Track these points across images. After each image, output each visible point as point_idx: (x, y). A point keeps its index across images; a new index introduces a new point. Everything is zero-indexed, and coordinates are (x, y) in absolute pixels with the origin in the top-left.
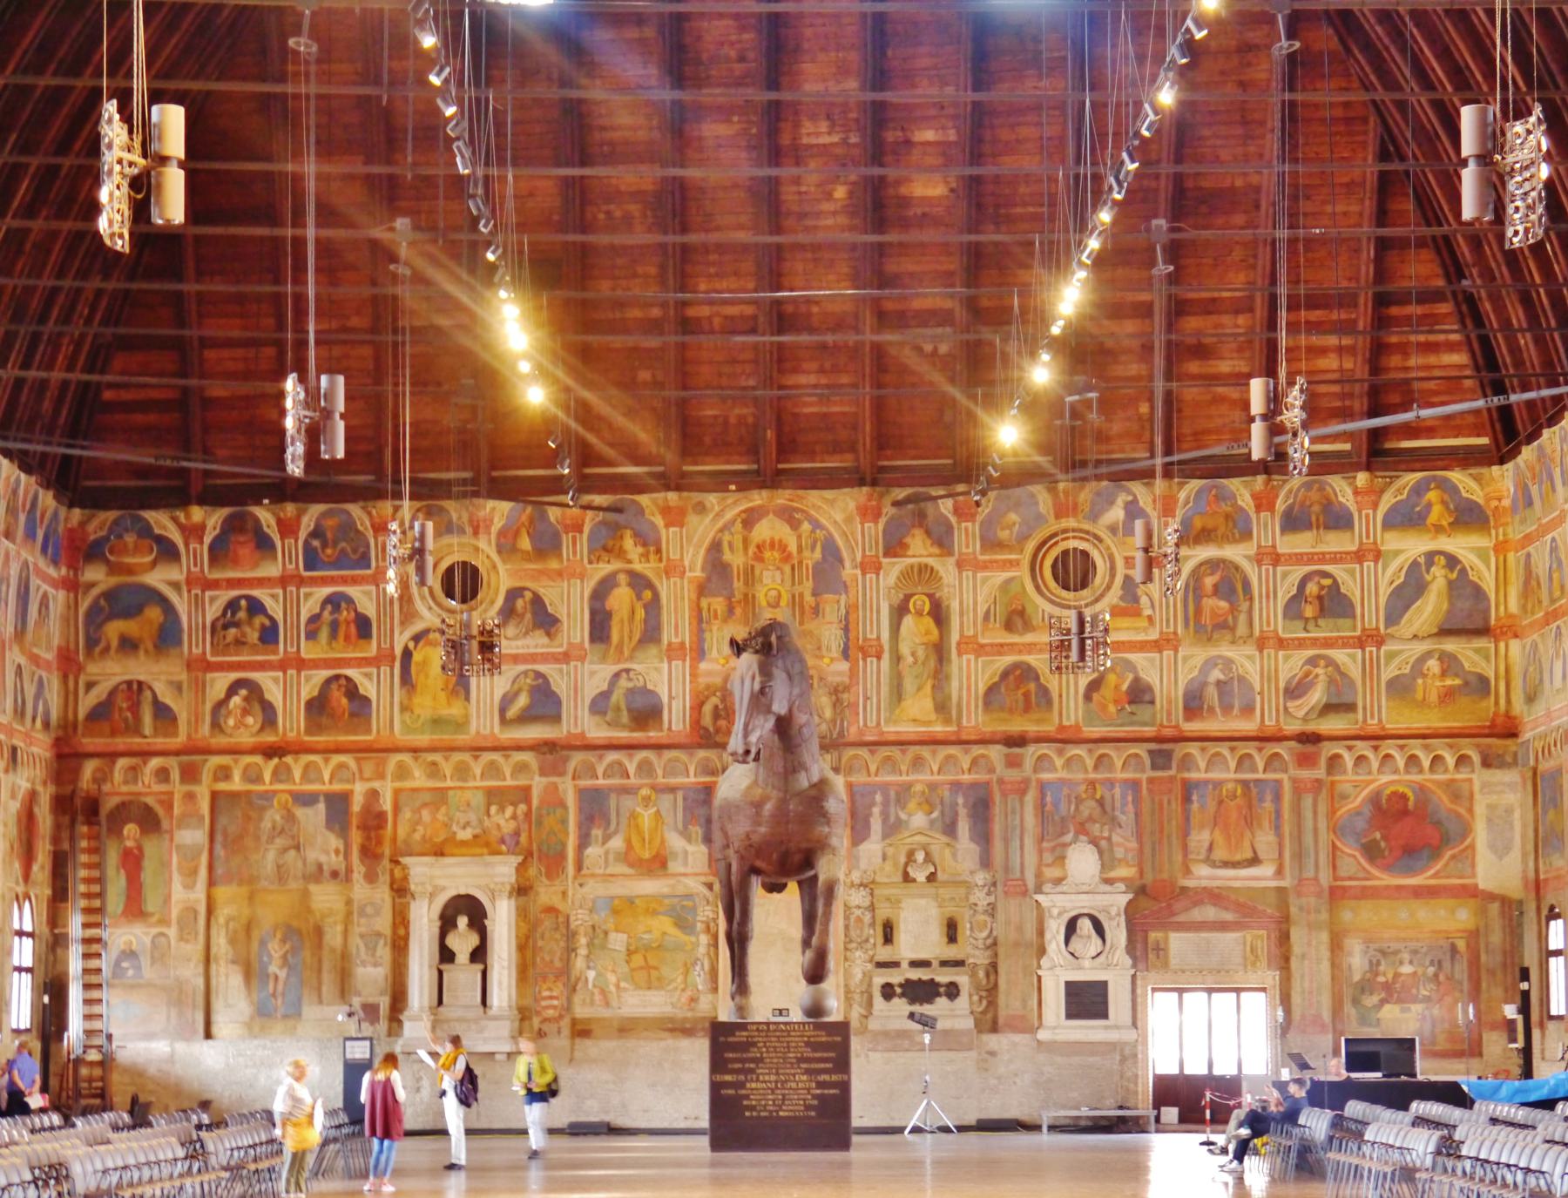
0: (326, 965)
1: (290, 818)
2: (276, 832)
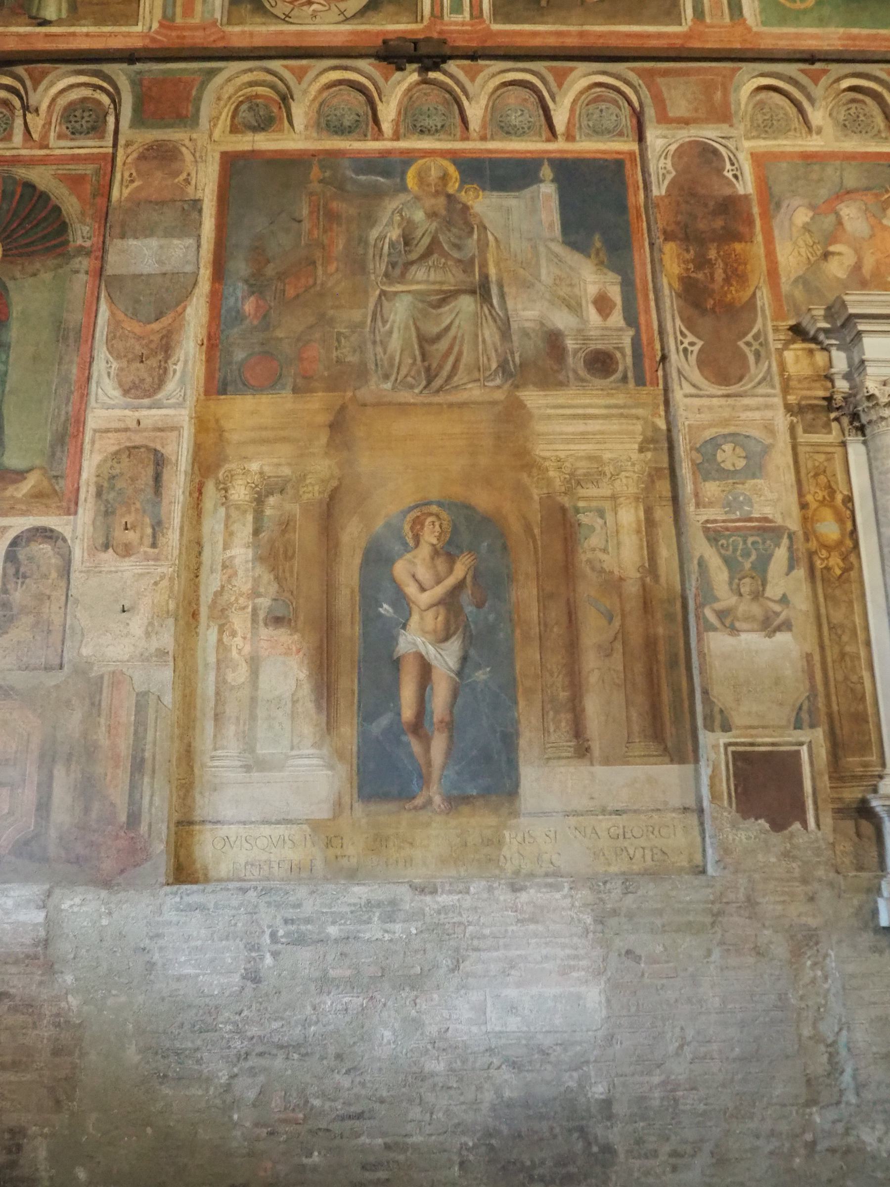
0: (594, 631)
1: (457, 216)
2: (408, 253)
